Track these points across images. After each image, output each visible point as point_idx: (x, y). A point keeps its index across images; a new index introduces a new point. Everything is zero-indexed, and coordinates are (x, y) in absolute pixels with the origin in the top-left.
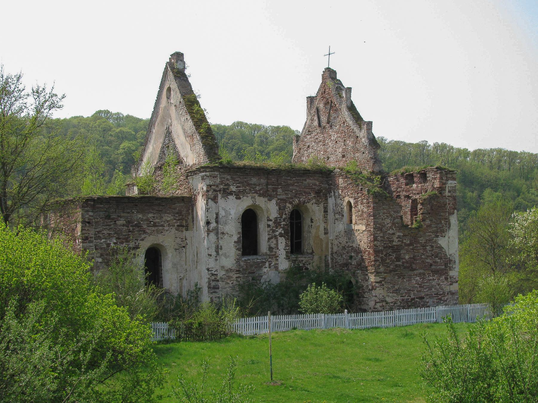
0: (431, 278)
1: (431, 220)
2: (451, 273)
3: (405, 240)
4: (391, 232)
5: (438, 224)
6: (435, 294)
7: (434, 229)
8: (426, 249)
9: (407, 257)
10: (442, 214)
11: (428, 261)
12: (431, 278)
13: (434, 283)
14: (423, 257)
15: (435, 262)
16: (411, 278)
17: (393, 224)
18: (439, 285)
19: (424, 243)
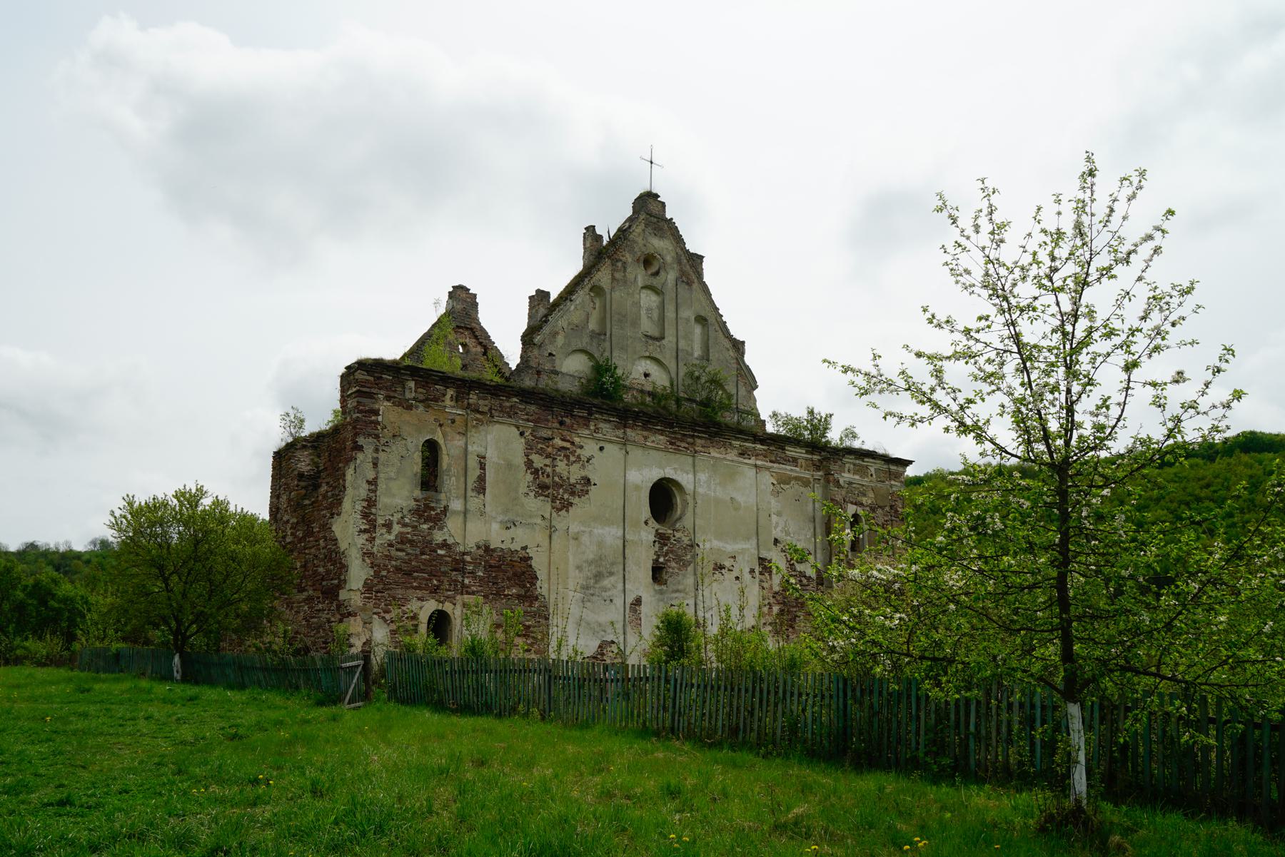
0: (320, 606)
1: (328, 483)
2: (343, 595)
3: (299, 530)
4: (284, 519)
5: (335, 488)
6: (324, 643)
7: (330, 500)
8: (319, 545)
9: (298, 565)
10: (340, 465)
11: (321, 570)
12: (320, 606)
13: (324, 616)
14: (315, 562)
15: (328, 572)
16: (300, 606)
17: (289, 500)
18: (329, 621)
19: (319, 532)
